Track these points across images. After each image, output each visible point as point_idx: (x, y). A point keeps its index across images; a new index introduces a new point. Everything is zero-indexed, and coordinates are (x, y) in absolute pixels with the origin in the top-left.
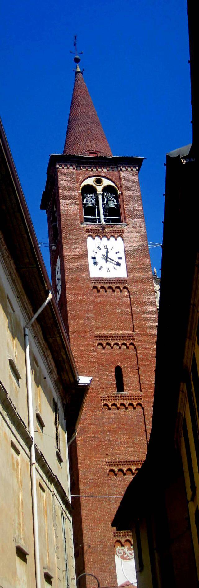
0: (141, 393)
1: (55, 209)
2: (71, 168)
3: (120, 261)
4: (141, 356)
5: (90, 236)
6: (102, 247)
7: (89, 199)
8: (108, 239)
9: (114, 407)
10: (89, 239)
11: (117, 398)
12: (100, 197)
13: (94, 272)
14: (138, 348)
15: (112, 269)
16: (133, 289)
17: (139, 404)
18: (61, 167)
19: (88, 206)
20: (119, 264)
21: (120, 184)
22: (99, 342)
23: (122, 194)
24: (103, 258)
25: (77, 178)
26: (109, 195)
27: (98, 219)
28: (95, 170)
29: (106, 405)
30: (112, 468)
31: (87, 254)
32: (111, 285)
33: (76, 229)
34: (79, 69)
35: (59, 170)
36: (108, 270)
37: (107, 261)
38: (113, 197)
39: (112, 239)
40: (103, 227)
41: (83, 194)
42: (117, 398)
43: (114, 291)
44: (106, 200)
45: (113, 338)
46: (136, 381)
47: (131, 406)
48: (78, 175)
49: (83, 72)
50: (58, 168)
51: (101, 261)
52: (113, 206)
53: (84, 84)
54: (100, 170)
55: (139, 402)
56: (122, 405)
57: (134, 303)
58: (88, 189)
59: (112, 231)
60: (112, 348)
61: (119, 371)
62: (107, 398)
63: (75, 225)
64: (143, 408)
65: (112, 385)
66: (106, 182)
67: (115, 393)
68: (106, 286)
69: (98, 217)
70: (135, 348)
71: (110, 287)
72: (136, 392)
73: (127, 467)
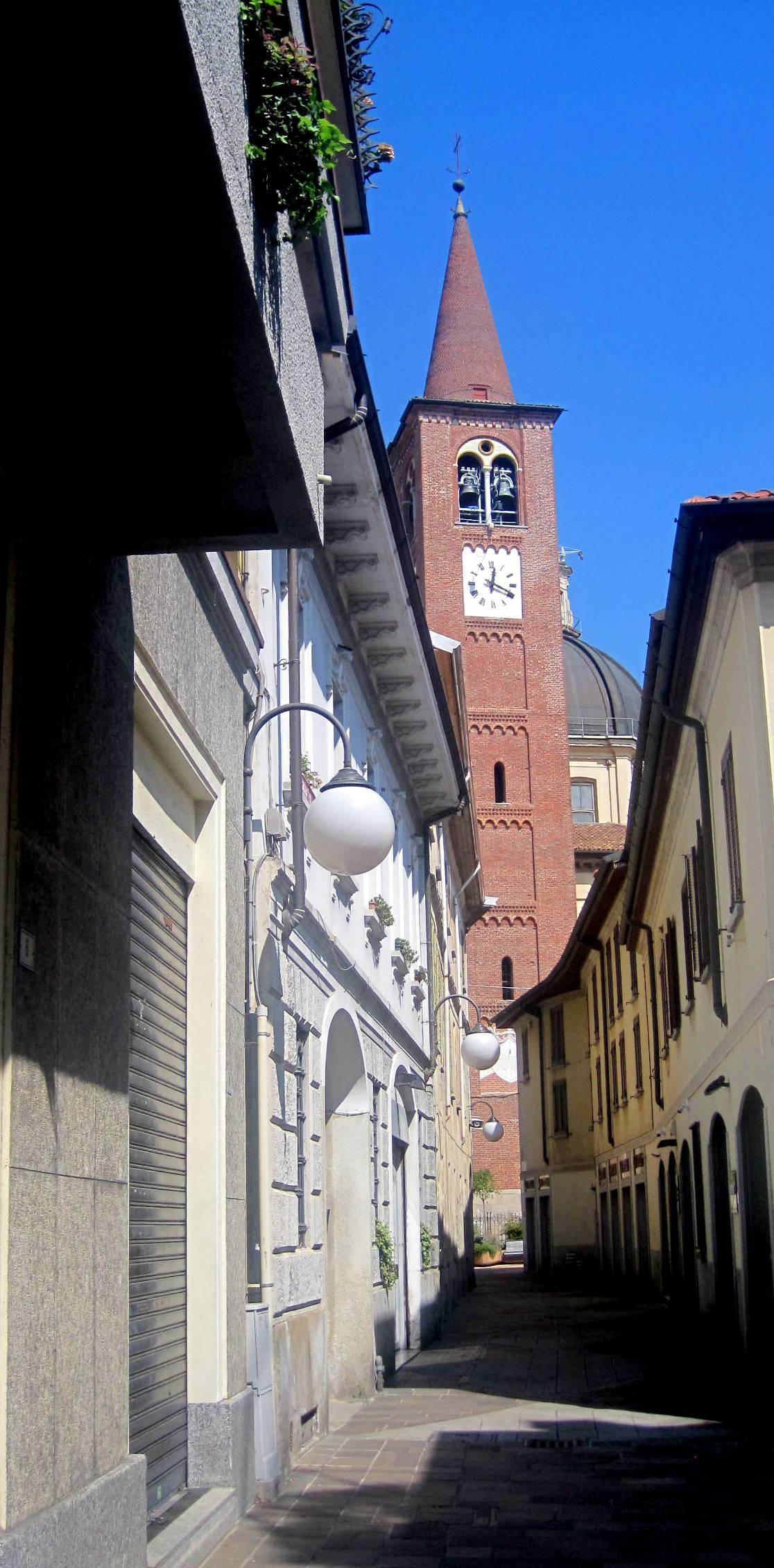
0: (531, 806)
1: (409, 479)
2: (443, 421)
3: (513, 590)
4: (535, 748)
5: (468, 545)
6: (486, 565)
7: (469, 477)
8: (497, 552)
9: (490, 825)
10: (467, 550)
11: (494, 812)
12: (487, 475)
13: (472, 608)
17: (527, 822)
18: (427, 420)
19: (465, 491)
20: (511, 595)
21: (522, 452)
23: (523, 472)
24: (486, 585)
25: (451, 442)
26: (503, 470)
27: (482, 513)
28: (481, 425)
31: (462, 577)
33: (445, 532)
34: (461, 210)
35: (423, 425)
36: (493, 605)
37: (492, 589)
38: (508, 474)
39: (502, 551)
40: (490, 532)
41: (459, 468)
42: (494, 812)
43: (500, 641)
45: (495, 718)
46: (525, 786)
47: (514, 825)
48: (453, 433)
49: (469, 215)
50: (421, 422)
51: (483, 591)
52: (508, 494)
53: (470, 241)
54: (490, 426)
55: (527, 818)
56: (502, 822)
57: (530, 662)
58: (469, 461)
60: (492, 733)
62: (481, 811)
63: (444, 525)
64: (531, 829)
65: (488, 790)
66: (499, 449)
68: (489, 632)
69: (482, 511)
70: (527, 734)
71: (495, 635)
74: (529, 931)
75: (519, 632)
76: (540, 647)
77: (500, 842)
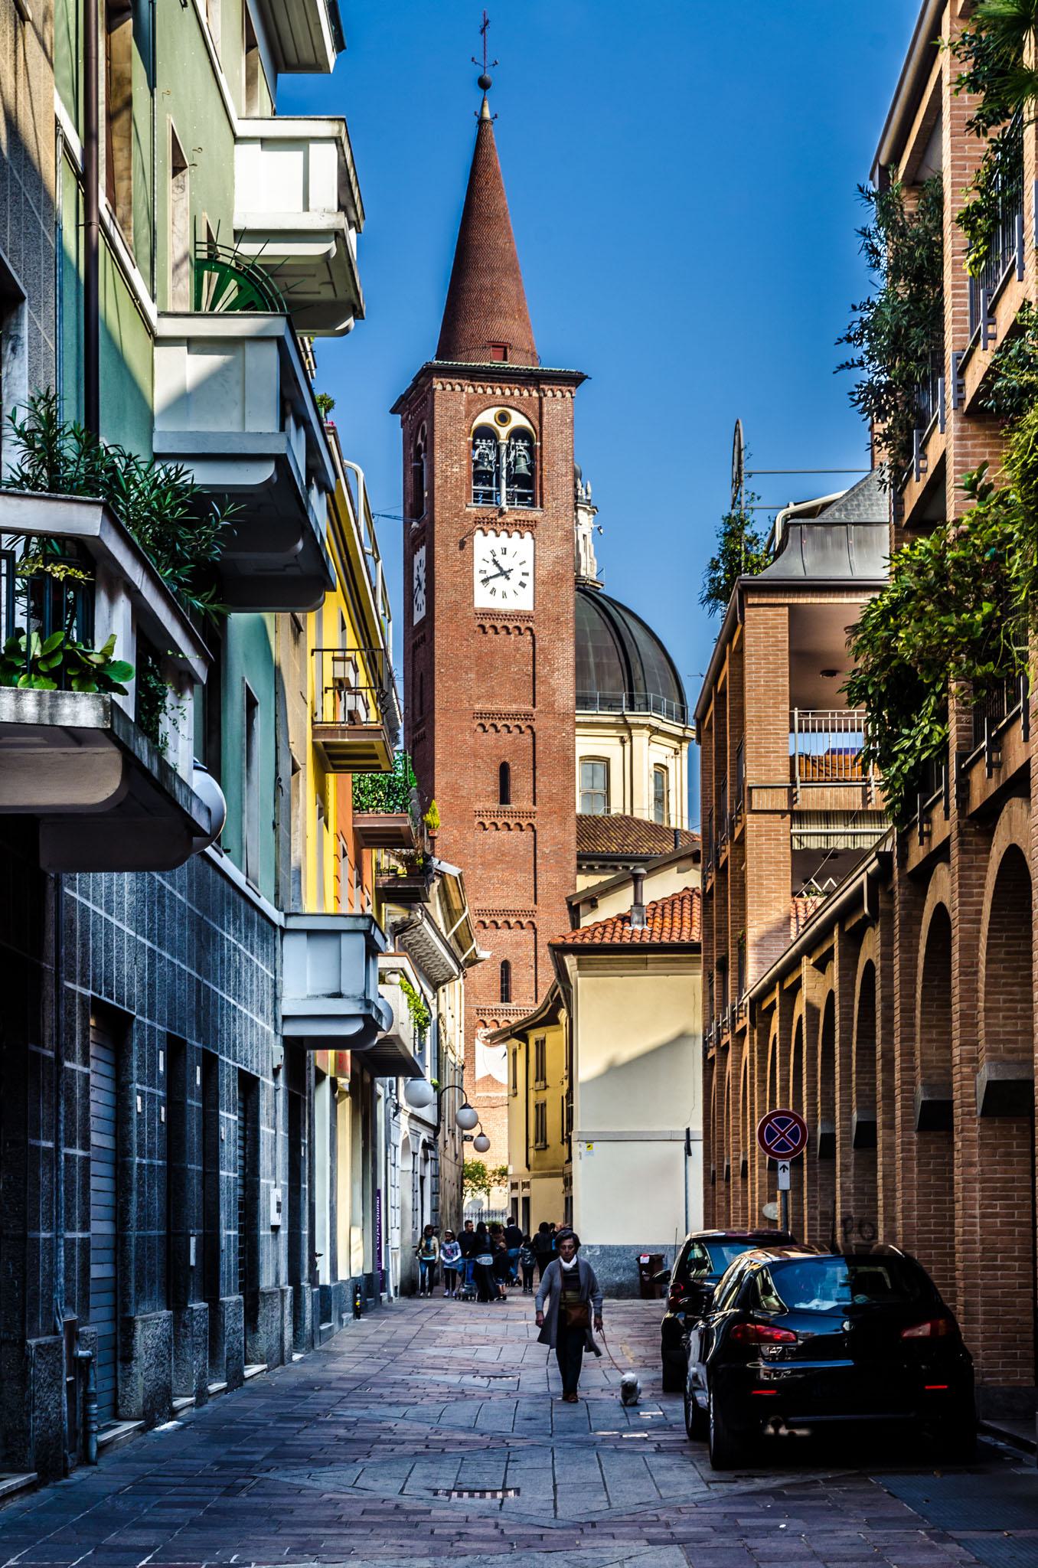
0: (535, 809)
3: (525, 579)
5: (481, 529)
10: (479, 533)
11: (499, 814)
13: (483, 599)
14: (538, 734)
15: (510, 594)
16: (542, 634)
20: (522, 585)
22: (479, 721)
29: (482, 823)
30: (482, 919)
32: (506, 623)
33: (457, 515)
35: (437, 394)
36: (504, 595)
41: (474, 441)
43: (509, 633)
44: (513, 454)
45: (502, 716)
55: (531, 821)
57: (540, 658)
58: (485, 433)
59: (516, 523)
61: (504, 770)
63: (456, 507)
64: (534, 831)
66: (517, 420)
67: (496, 806)
68: (499, 624)
70: (534, 733)
71: (506, 628)
72: (526, 805)
73: (504, 918)
74: (527, 935)
75: (531, 624)
76: (551, 641)
77: (503, 844)
